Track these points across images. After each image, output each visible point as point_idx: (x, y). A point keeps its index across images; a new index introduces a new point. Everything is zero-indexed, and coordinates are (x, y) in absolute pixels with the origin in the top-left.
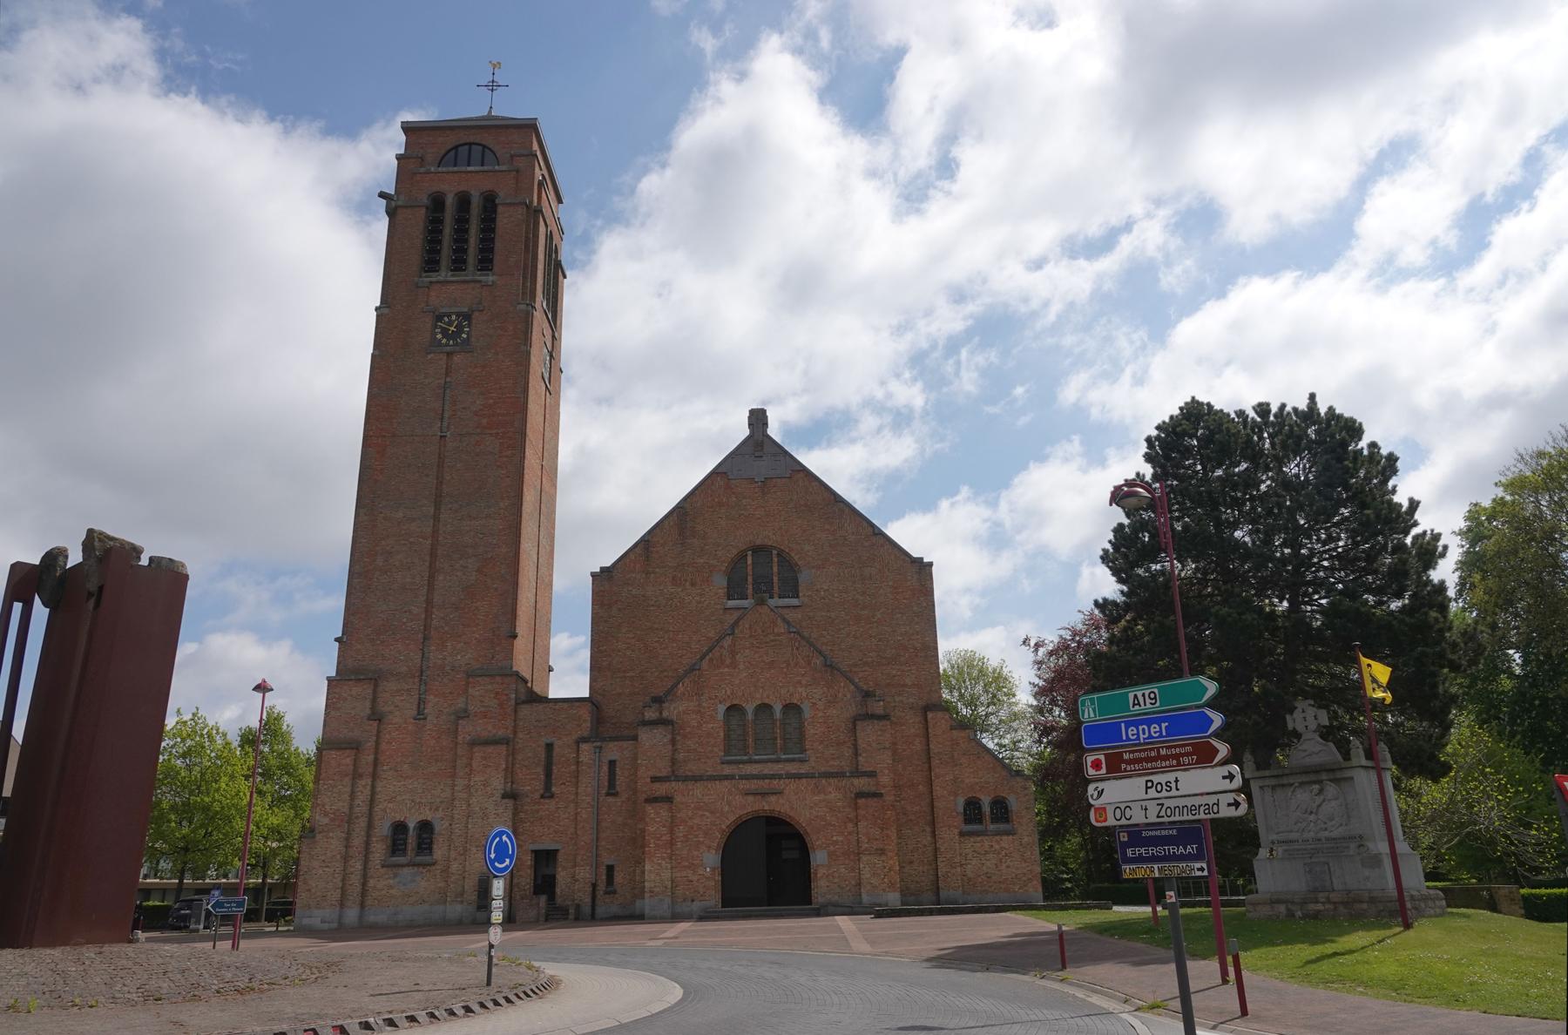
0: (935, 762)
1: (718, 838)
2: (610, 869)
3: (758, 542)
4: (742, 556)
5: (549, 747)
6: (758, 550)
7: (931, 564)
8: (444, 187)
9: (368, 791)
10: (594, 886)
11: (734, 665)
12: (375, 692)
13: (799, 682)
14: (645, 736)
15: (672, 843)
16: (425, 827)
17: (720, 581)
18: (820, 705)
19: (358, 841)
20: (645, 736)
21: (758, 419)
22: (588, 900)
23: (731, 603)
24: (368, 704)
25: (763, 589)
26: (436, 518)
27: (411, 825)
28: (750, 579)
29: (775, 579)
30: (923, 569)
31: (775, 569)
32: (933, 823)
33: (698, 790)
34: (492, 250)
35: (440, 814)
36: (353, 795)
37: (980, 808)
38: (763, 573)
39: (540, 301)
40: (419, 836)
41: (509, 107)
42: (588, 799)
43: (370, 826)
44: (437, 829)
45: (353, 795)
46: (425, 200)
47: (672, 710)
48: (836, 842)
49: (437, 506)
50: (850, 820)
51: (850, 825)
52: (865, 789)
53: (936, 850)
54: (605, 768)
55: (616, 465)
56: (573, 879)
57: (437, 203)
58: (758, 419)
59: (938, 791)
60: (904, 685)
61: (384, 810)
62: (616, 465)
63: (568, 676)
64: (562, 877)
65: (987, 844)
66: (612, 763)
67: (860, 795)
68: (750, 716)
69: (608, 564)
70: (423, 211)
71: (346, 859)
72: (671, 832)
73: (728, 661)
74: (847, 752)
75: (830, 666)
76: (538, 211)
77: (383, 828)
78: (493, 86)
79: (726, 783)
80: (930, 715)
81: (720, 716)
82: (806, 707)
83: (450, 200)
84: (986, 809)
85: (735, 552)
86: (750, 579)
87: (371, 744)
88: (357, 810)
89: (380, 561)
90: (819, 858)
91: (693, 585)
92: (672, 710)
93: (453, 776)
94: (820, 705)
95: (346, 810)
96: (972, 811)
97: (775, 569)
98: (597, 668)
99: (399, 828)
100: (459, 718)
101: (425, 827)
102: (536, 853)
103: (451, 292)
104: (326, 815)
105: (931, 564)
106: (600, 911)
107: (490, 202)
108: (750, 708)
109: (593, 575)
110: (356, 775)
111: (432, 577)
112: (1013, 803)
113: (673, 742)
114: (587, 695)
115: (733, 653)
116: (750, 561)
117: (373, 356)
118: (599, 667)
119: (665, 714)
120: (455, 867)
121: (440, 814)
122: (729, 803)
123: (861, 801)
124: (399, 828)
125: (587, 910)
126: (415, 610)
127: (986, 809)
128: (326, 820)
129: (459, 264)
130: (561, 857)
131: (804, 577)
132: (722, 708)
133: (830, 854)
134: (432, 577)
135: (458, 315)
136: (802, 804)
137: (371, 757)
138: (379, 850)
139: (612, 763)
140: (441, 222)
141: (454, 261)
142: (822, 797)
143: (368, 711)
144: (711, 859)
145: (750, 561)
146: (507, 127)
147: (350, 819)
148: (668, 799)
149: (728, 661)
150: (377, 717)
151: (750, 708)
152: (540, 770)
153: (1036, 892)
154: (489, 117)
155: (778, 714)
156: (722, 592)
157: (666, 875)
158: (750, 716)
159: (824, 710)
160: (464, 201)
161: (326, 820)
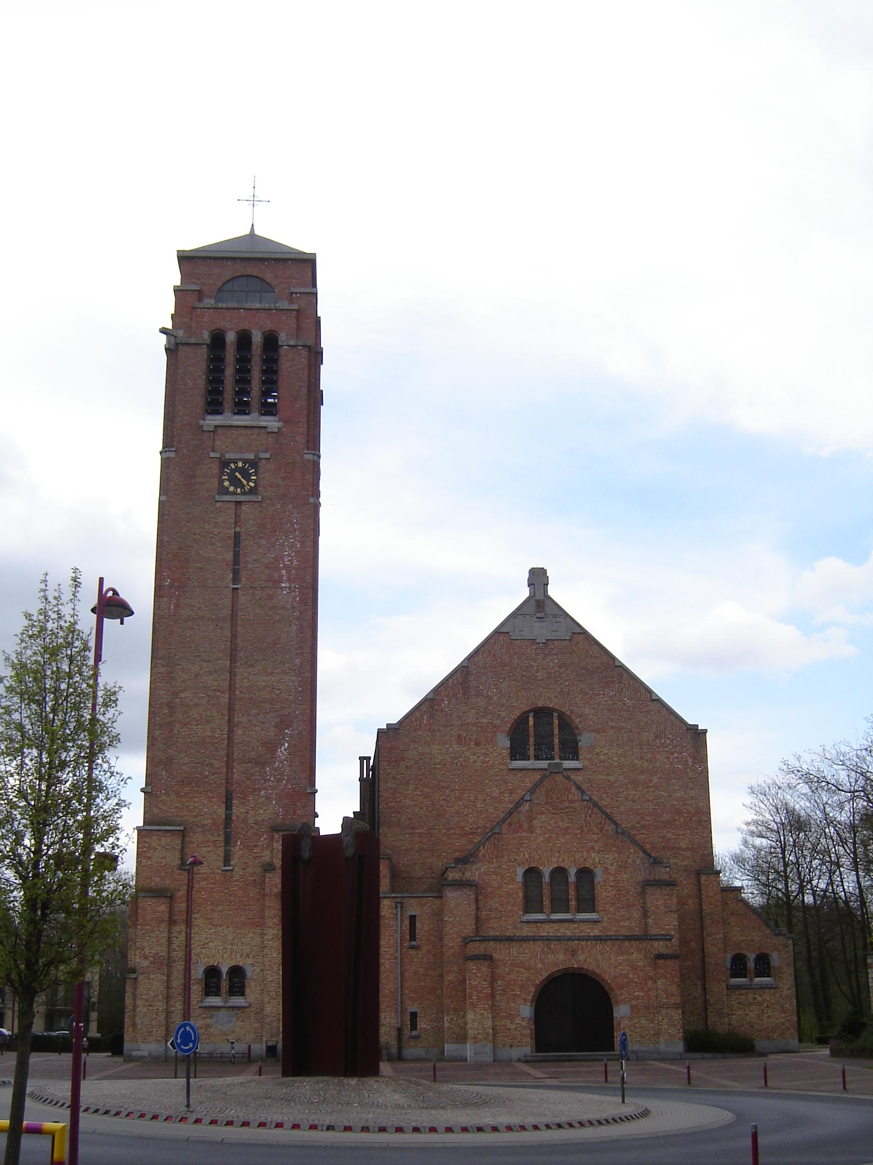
0: (707, 921)
2: (414, 1015)
3: (540, 704)
4: (524, 718)
6: (542, 713)
7: (705, 732)
8: (221, 324)
9: (182, 937)
10: (400, 1030)
11: (531, 830)
12: (183, 843)
13: (593, 848)
14: (451, 895)
15: (492, 996)
16: (237, 972)
17: (504, 742)
18: (612, 869)
19: (177, 982)
20: (451, 895)
21: (538, 578)
22: (394, 1043)
24: (178, 854)
26: (232, 673)
27: (224, 970)
28: (532, 740)
29: (556, 741)
31: (556, 731)
32: (704, 979)
33: (514, 949)
35: (249, 961)
36: (170, 941)
37: (745, 965)
38: (543, 733)
40: (230, 980)
42: (391, 951)
43: (188, 969)
44: (249, 974)
45: (170, 941)
46: (206, 337)
47: (474, 872)
48: (638, 997)
49: (233, 658)
50: (651, 978)
51: (650, 982)
52: (663, 951)
53: (706, 1002)
54: (407, 923)
57: (218, 340)
58: (538, 578)
60: (679, 848)
61: (198, 955)
65: (751, 996)
66: (413, 918)
67: (659, 956)
68: (547, 878)
69: (395, 720)
70: (204, 349)
71: (168, 998)
72: (492, 985)
73: (526, 827)
74: (637, 914)
75: (620, 832)
77: (198, 972)
78: (253, 201)
79: (540, 943)
80: (703, 878)
81: (519, 878)
83: (231, 337)
84: (751, 965)
85: (518, 713)
86: (532, 740)
87: (182, 892)
88: (174, 954)
90: (621, 1011)
91: (477, 744)
92: (474, 872)
94: (612, 869)
95: (164, 954)
96: (738, 966)
97: (556, 731)
99: (212, 972)
100: (266, 870)
101: (237, 972)
104: (146, 958)
105: (705, 732)
106: (408, 1052)
107: (271, 342)
108: (546, 872)
110: (172, 922)
111: (231, 731)
112: (775, 959)
113: (477, 901)
114: (323, 832)
115: (530, 818)
116: (531, 722)
117: (161, 503)
119: (468, 875)
121: (249, 961)
122: (542, 961)
123: (661, 962)
124: (212, 972)
125: (394, 1051)
126: (216, 764)
127: (751, 965)
128: (146, 963)
129: (242, 408)
131: (585, 740)
132: (520, 871)
133: (633, 1008)
134: (231, 731)
135: (245, 461)
136: (607, 964)
137: (183, 906)
138: (196, 990)
140: (222, 360)
141: (236, 404)
142: (625, 957)
143: (178, 862)
144: (527, 1010)
145: (531, 722)
147: (170, 963)
148: (487, 958)
149: (526, 827)
150: (189, 866)
151: (546, 872)
155: (572, 878)
156: (506, 753)
157: (489, 1024)
160: (244, 339)
161: (146, 963)
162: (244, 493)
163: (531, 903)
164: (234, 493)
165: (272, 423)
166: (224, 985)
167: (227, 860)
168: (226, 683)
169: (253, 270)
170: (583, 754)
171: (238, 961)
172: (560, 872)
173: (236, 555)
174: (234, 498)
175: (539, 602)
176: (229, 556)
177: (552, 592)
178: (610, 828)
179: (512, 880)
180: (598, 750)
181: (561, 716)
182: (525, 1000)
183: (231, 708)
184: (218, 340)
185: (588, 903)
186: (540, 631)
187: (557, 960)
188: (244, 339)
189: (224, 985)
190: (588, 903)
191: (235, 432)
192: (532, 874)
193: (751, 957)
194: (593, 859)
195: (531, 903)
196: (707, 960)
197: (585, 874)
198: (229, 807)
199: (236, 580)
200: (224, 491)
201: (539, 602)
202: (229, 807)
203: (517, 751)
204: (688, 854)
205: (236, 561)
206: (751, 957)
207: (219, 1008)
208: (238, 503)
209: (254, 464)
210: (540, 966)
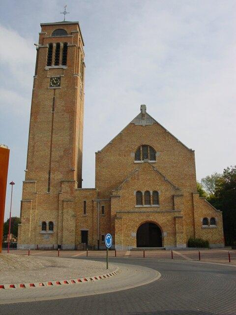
1: (136, 229)
5: (85, 202)
6: (144, 146)
10: (98, 241)
11: (138, 179)
16: (51, 223)
17: (133, 155)
21: (143, 108)
22: (97, 245)
23: (136, 162)
25: (145, 156)
27: (47, 223)
30: (192, 152)
34: (66, 59)
39: (80, 73)
41: (69, 19)
44: (54, 224)
54: (101, 208)
55: (100, 120)
56: (92, 239)
57: (51, 46)
58: (143, 108)
59: (196, 216)
62: (100, 120)
63: (89, 181)
64: (90, 239)
66: (103, 207)
68: (143, 194)
69: (100, 150)
74: (171, 205)
76: (79, 48)
78: (65, 13)
82: (159, 192)
84: (209, 221)
85: (136, 147)
89: (36, 149)
90: (165, 234)
93: (58, 209)
96: (205, 221)
97: (149, 152)
98: (97, 179)
99: (44, 223)
101: (51, 223)
102: (82, 231)
103: (53, 71)
106: (100, 248)
109: (96, 153)
112: (216, 219)
116: (141, 149)
118: (97, 179)
120: (59, 234)
124: (44, 223)
125: (97, 247)
127: (209, 221)
129: (57, 63)
130: (89, 233)
131: (157, 155)
133: (168, 233)
139: (103, 207)
144: (134, 234)
146: (70, 24)
152: (83, 208)
153: (223, 245)
154: (64, 22)
155: (151, 194)
156: (133, 158)
158: (143, 194)
159: (164, 194)
160: (58, 45)
162: (57, 86)
163: (139, 202)
164: (53, 86)
165: (65, 67)
166: (48, 227)
167: (49, 191)
168: (50, 140)
169: (62, 28)
170: (157, 158)
171: (52, 220)
172: (147, 192)
173: (54, 103)
174: (54, 88)
175: (143, 115)
176: (52, 104)
177: (147, 111)
178: (163, 179)
179: (132, 195)
180: (161, 157)
181: (151, 147)
182: (133, 231)
183: (51, 147)
184: (51, 46)
185: (157, 202)
186: (144, 123)
187: (144, 219)
188: (58, 45)
189: (48, 227)
190: (157, 202)
191: (54, 70)
192: (139, 193)
193: (209, 219)
194: (157, 188)
195: (139, 202)
196: (195, 220)
197: (156, 193)
198: (49, 175)
199: (53, 110)
200: (51, 86)
201: (143, 115)
202: (49, 175)
203: (137, 157)
204: (189, 187)
205: (53, 105)
206: (209, 219)
207: (45, 234)
208: (55, 89)
209: (59, 78)
210: (138, 220)
